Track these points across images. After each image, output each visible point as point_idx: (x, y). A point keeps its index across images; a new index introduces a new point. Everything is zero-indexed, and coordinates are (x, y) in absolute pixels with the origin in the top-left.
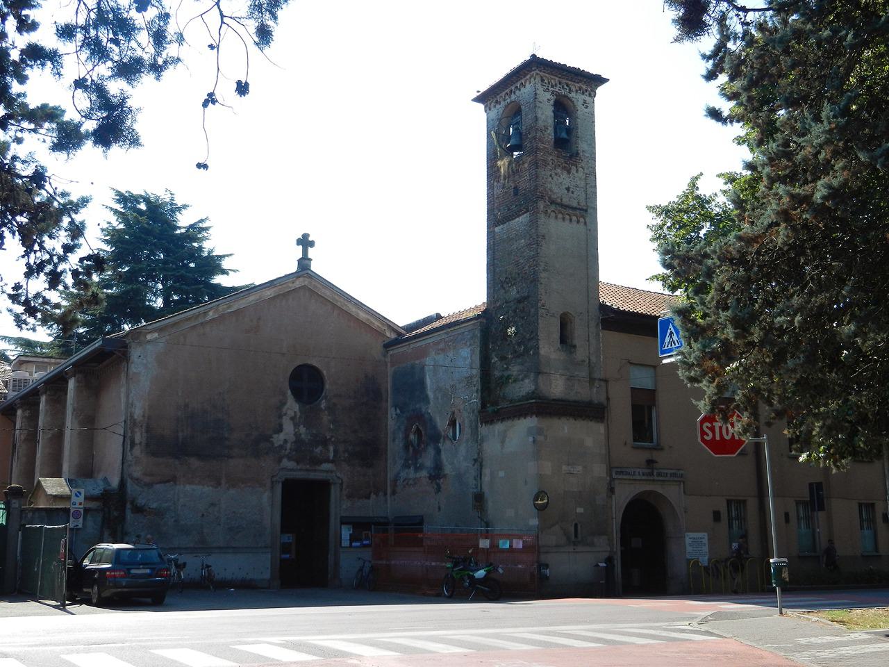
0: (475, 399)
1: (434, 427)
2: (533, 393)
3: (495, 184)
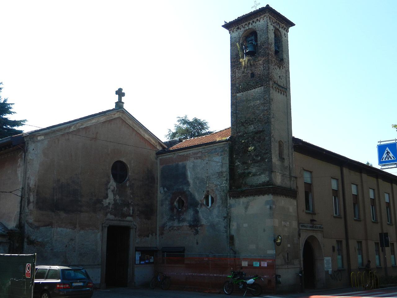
0: (225, 184)
1: (194, 199)
2: (268, 182)
3: (237, 71)
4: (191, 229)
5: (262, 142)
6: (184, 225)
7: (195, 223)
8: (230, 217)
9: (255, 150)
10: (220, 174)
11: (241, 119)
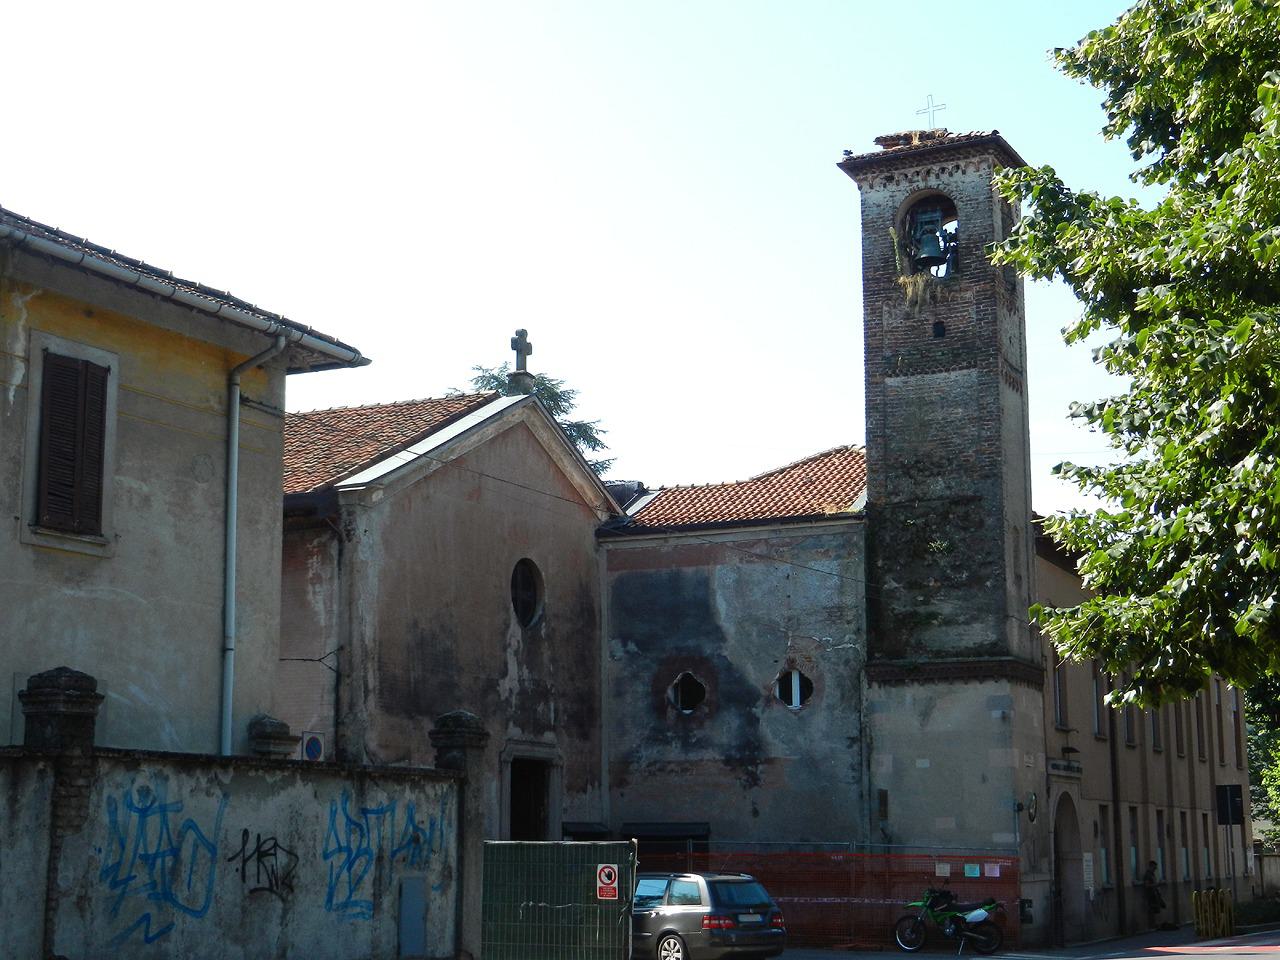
0: (852, 643)
1: (740, 680)
2: (994, 644)
3: (885, 308)
4: (731, 770)
5: (972, 530)
6: (706, 758)
7: (747, 753)
8: (871, 739)
9: (950, 550)
10: (835, 614)
11: (900, 456)
